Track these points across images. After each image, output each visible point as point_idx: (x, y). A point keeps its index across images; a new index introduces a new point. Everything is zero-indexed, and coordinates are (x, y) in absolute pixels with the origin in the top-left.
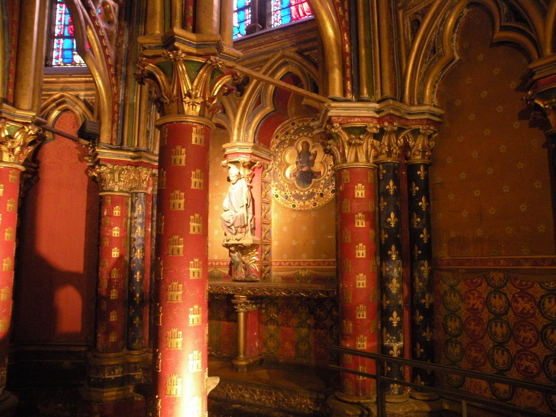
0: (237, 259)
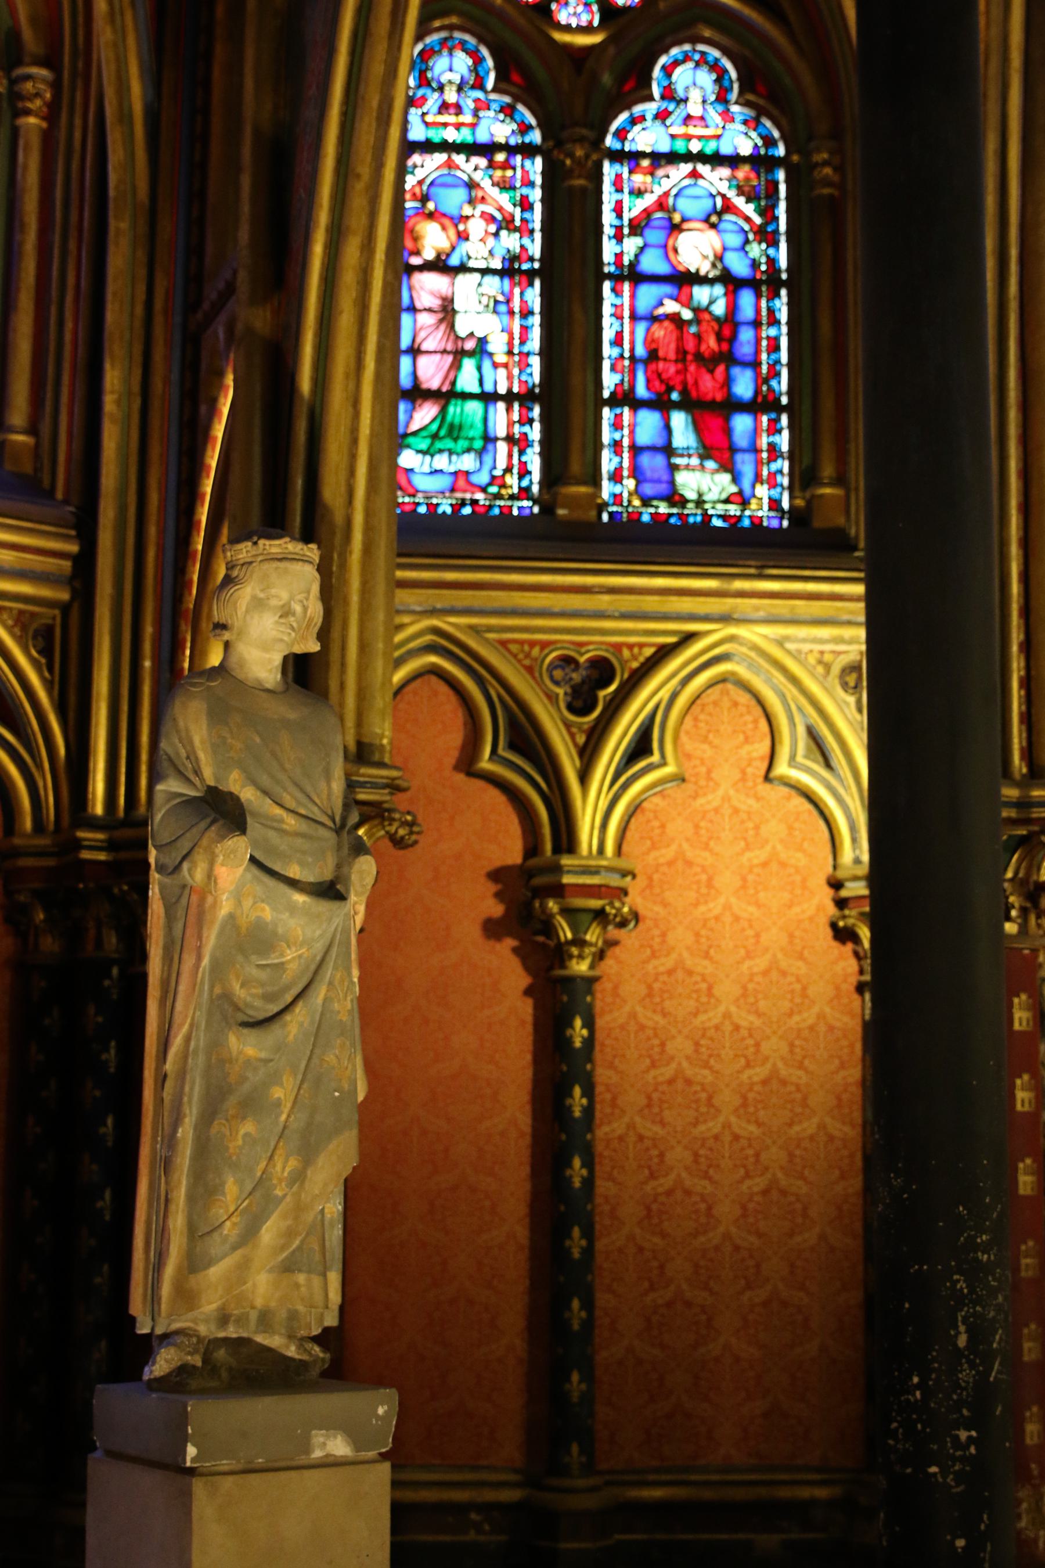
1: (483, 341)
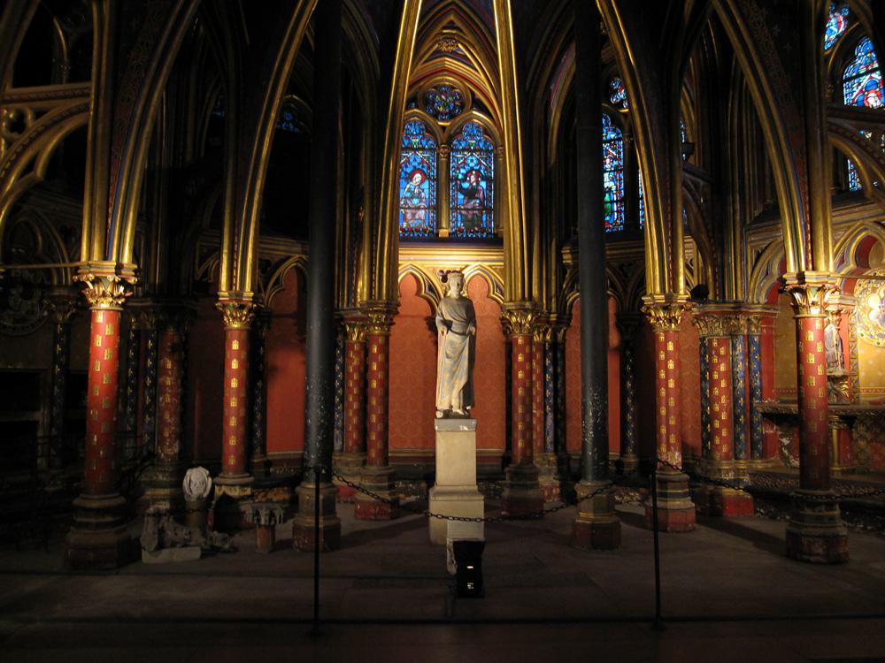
0: (830, 387)
1: (611, 188)
